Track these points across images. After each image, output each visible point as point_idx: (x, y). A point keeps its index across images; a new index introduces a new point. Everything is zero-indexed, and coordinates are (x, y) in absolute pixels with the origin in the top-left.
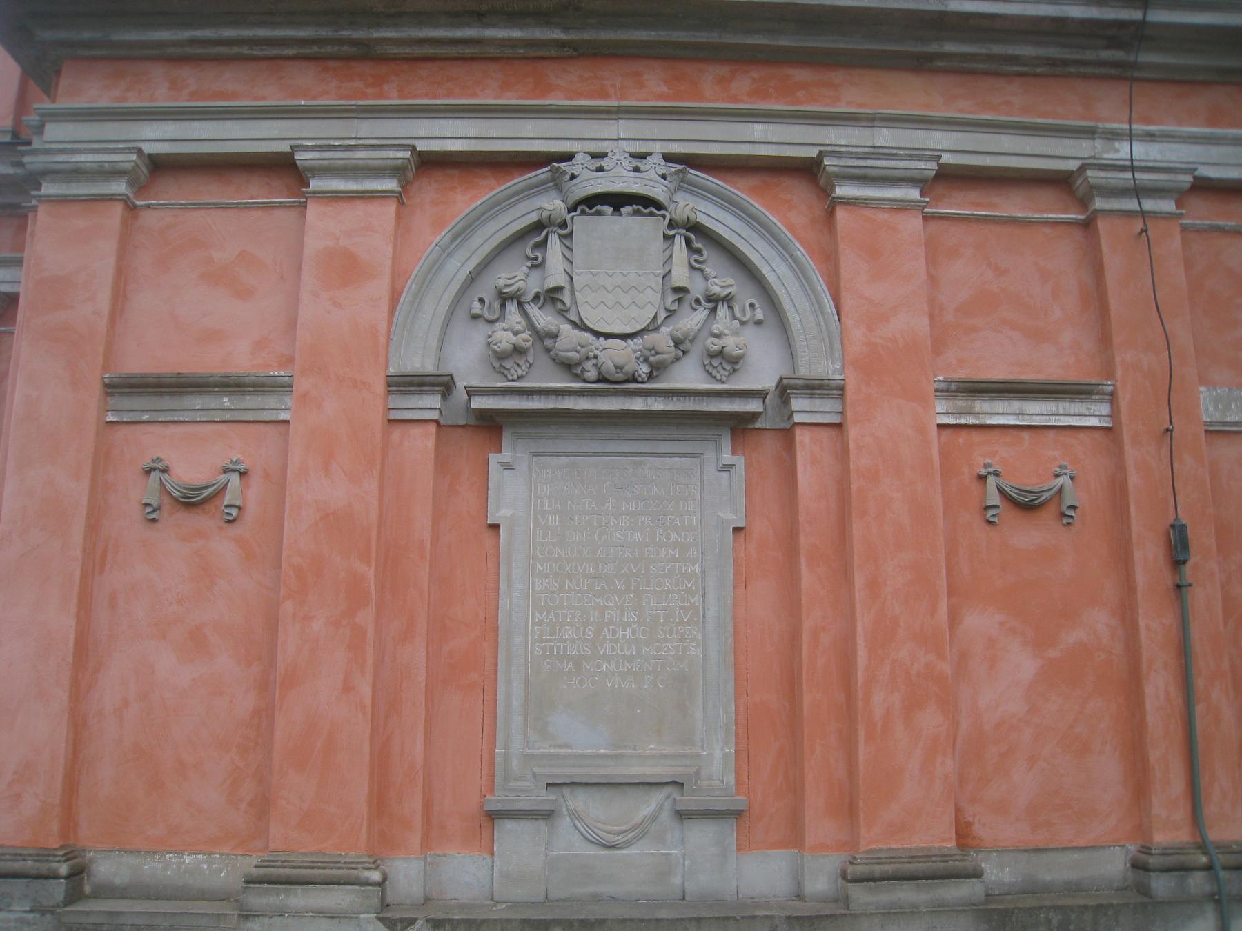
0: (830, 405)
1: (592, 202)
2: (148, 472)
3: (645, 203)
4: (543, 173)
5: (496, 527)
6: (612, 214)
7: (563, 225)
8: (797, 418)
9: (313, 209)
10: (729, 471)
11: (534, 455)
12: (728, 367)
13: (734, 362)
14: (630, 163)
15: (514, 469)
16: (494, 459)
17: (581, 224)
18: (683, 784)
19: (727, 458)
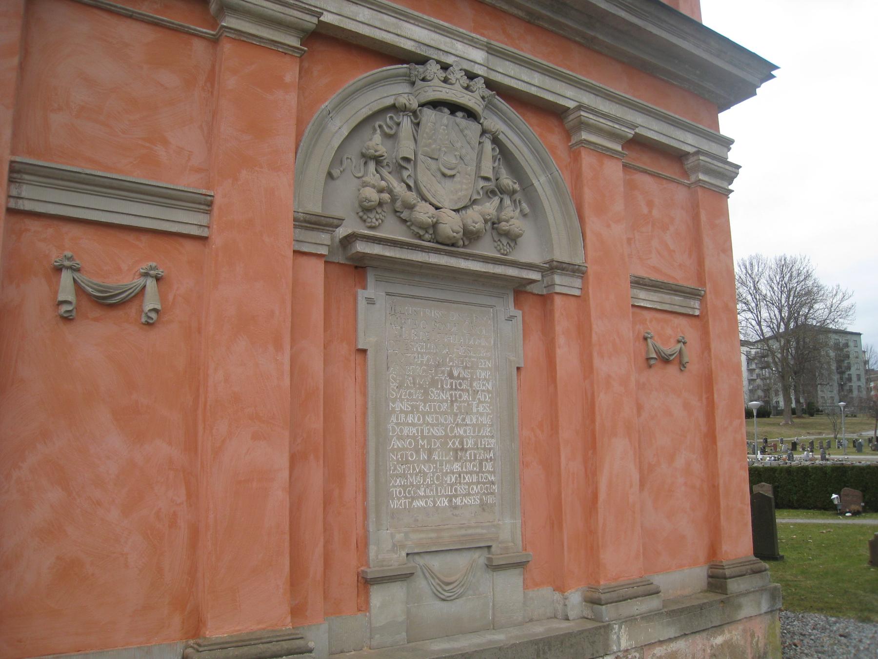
2: (679, 342)
4: (403, 68)
5: (364, 351)
6: (462, 118)
7: (414, 113)
8: (558, 289)
9: (227, 47)
10: (512, 320)
11: (387, 295)
12: (512, 245)
13: (513, 238)
14: (465, 81)
15: (374, 304)
16: (362, 294)
17: (429, 116)
18: (489, 547)
19: (512, 310)
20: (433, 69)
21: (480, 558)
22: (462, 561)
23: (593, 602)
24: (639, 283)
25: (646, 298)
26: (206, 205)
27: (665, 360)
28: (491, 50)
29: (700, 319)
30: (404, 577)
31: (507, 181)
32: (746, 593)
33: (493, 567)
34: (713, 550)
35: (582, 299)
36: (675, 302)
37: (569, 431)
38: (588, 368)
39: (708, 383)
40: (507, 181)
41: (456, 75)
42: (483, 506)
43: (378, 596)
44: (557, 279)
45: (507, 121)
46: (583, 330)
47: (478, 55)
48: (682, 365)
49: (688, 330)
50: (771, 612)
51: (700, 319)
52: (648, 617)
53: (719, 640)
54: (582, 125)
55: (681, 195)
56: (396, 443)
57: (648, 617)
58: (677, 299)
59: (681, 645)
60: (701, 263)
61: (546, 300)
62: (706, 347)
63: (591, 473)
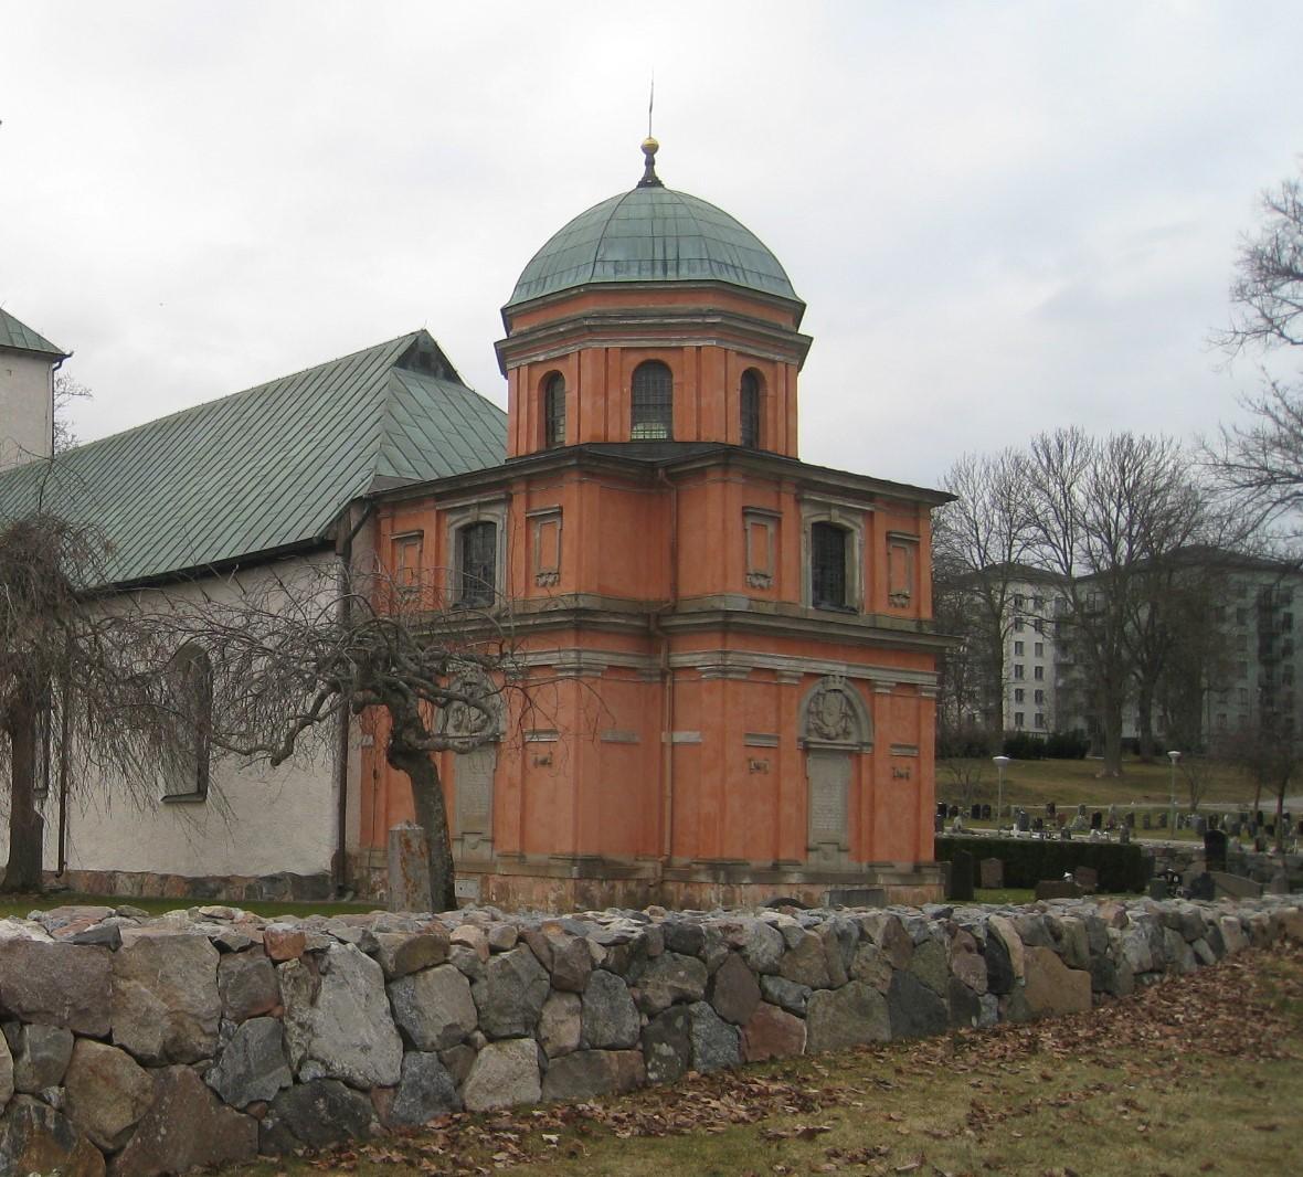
0: (870, 748)
1: (830, 691)
3: (840, 691)
4: (821, 680)
20: (831, 678)
21: (835, 847)
22: (831, 847)
23: (871, 866)
24: (894, 746)
25: (896, 752)
26: (778, 738)
27: (901, 777)
28: (849, 666)
29: (917, 758)
30: (816, 850)
31: (850, 713)
32: (929, 874)
33: (840, 850)
34: (917, 856)
35: (872, 754)
36: (906, 751)
37: (865, 806)
38: (872, 782)
39: (918, 787)
40: (850, 713)
41: (838, 679)
42: (837, 830)
43: (811, 855)
44: (865, 748)
45: (851, 689)
46: (872, 766)
47: (844, 668)
48: (908, 778)
49: (912, 763)
50: (939, 884)
51: (917, 758)
52: (892, 875)
53: (916, 890)
54: (876, 686)
55: (913, 702)
56: (814, 807)
57: (892, 875)
58: (908, 750)
59: (901, 888)
60: (919, 732)
61: (858, 755)
62: (919, 772)
63: (872, 821)
